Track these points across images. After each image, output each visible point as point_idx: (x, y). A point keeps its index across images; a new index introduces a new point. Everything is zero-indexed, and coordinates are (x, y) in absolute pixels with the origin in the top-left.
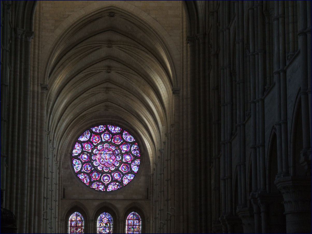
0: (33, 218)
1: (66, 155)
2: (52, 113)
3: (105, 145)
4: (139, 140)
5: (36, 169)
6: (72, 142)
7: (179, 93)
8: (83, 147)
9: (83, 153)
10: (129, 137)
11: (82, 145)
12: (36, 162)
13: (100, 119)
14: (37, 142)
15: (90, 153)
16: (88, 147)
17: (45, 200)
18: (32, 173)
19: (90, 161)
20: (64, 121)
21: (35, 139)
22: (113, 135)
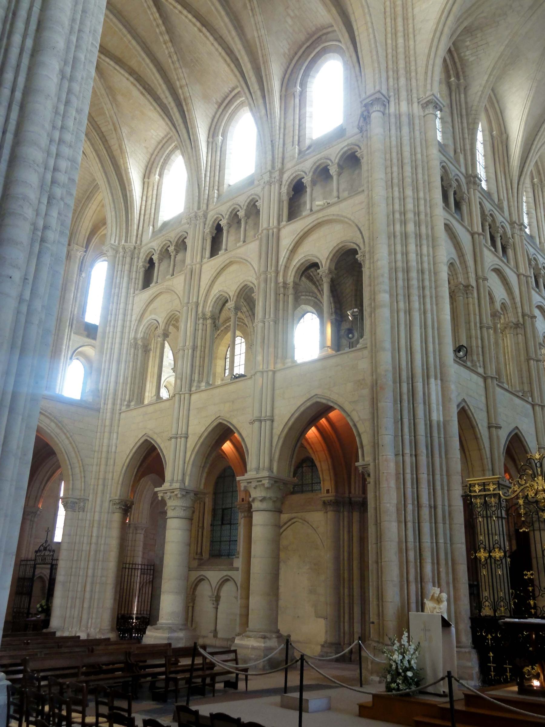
0: (419, 386)
12: (420, 255)
14: (417, 214)
21: (410, 206)
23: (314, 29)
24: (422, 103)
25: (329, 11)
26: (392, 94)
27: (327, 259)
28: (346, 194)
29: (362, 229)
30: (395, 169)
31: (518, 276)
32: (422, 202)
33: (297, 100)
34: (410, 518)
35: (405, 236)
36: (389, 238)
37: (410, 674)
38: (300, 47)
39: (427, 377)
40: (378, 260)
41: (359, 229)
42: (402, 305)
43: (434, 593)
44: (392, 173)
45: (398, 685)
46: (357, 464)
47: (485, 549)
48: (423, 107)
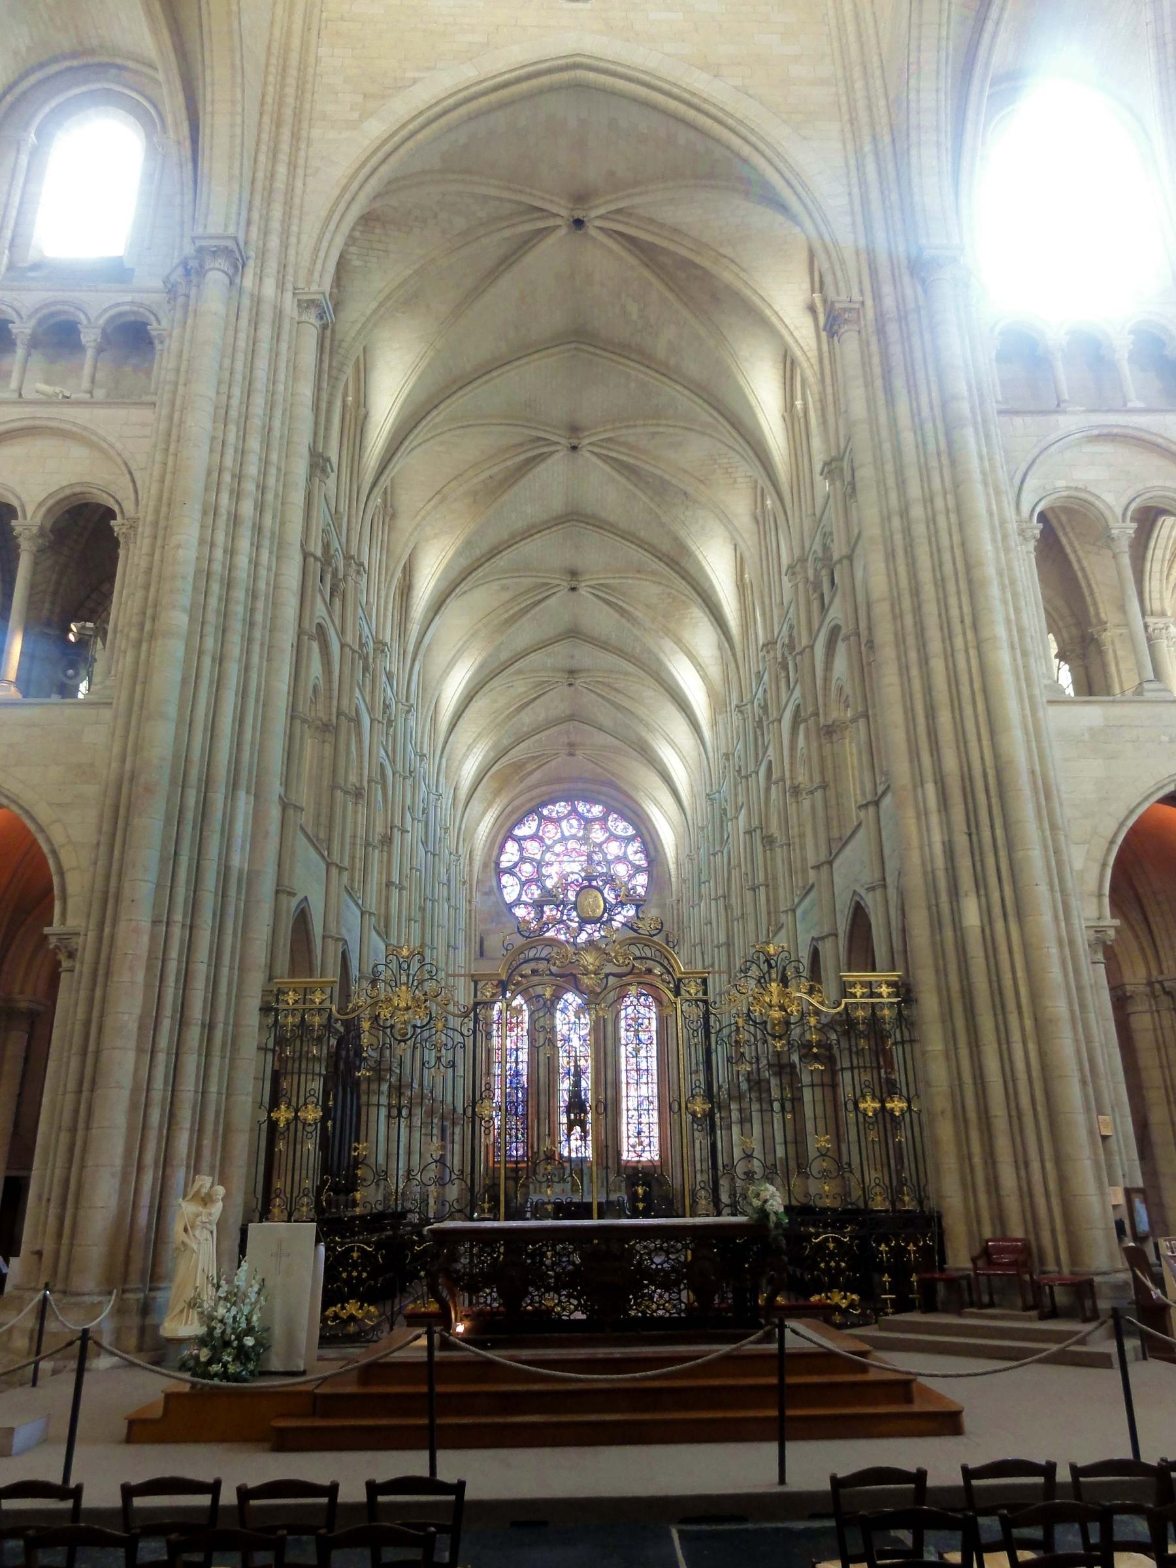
0: (218, 798)
1: (485, 865)
2: (420, 657)
3: (572, 844)
4: (644, 831)
5: (253, 594)
6: (500, 838)
7: (858, 322)
8: (521, 849)
9: (523, 860)
10: (622, 825)
11: (520, 845)
12: (255, 563)
13: (557, 787)
14: (262, 488)
15: (539, 863)
16: (533, 848)
17: (395, 893)
18: (227, 600)
19: (538, 879)
20: (470, 748)
21: (252, 469)
22: (587, 822)
23: (95, 42)
24: (301, 297)
25: (155, 32)
26: (252, 254)
27: (40, 505)
28: (100, 394)
29: (137, 475)
30: (237, 391)
31: (342, 646)
32: (273, 471)
33: (24, 159)
34: (163, 1043)
35: (235, 520)
36: (205, 513)
37: (249, 1341)
38: (55, 60)
39: (234, 785)
40: (178, 546)
41: (130, 473)
42: (209, 643)
43: (201, 1186)
44: (229, 397)
45: (225, 1366)
46: (47, 930)
47: (289, 1105)
48: (299, 305)
